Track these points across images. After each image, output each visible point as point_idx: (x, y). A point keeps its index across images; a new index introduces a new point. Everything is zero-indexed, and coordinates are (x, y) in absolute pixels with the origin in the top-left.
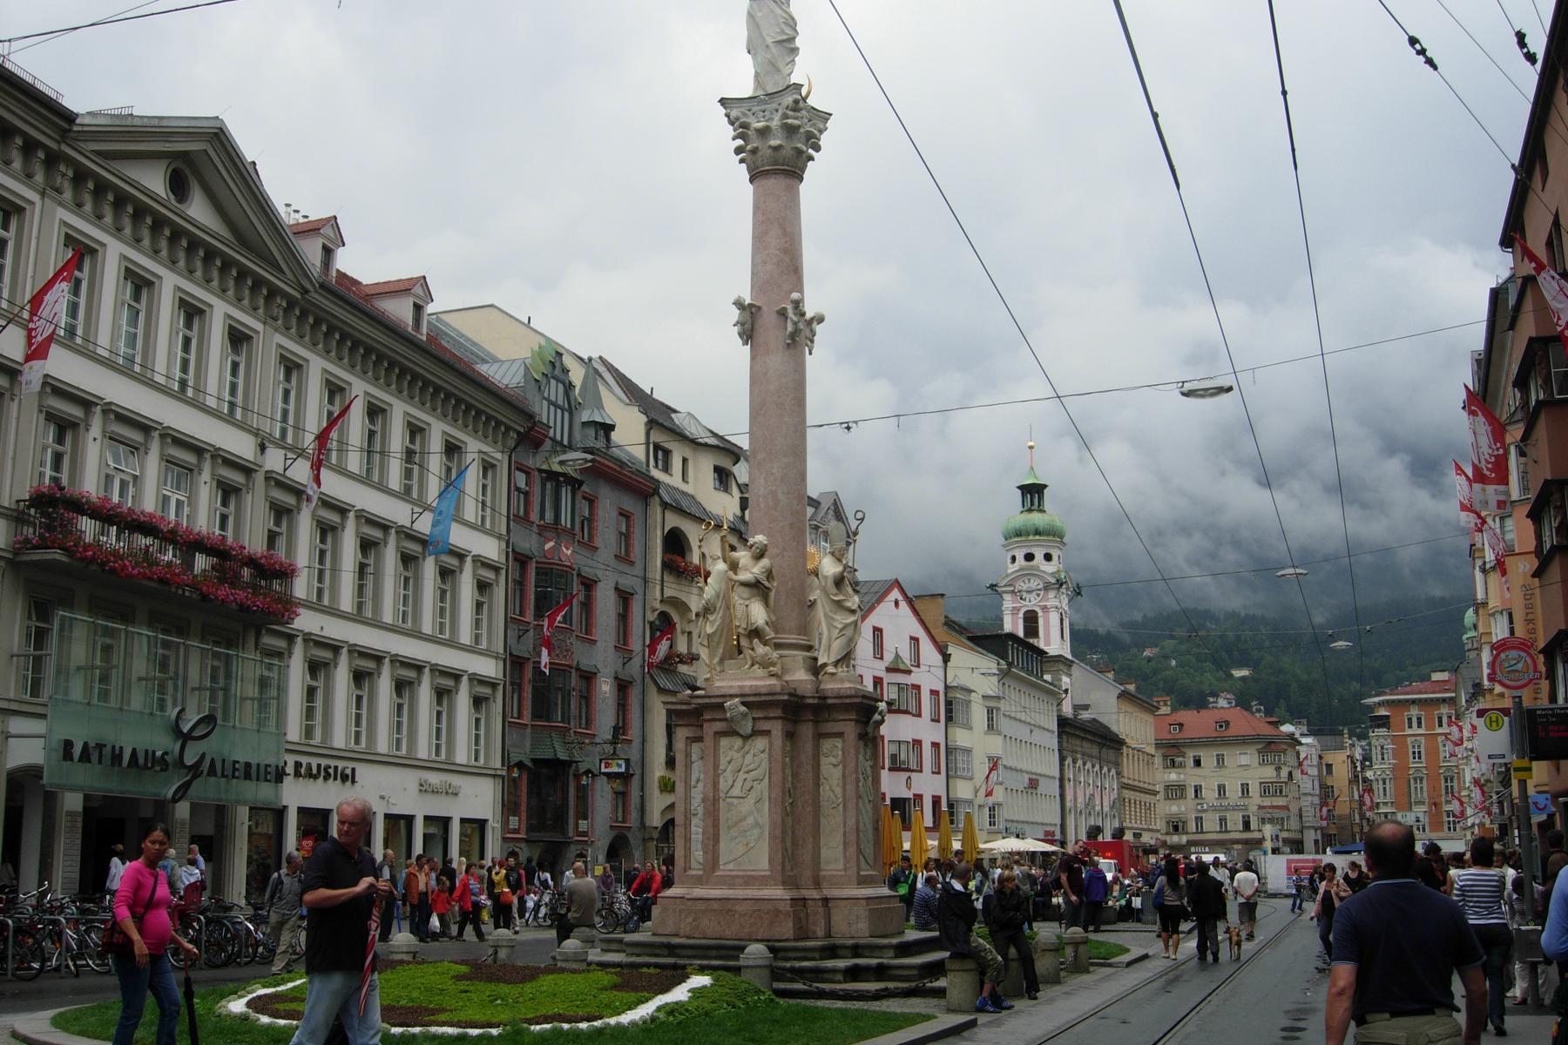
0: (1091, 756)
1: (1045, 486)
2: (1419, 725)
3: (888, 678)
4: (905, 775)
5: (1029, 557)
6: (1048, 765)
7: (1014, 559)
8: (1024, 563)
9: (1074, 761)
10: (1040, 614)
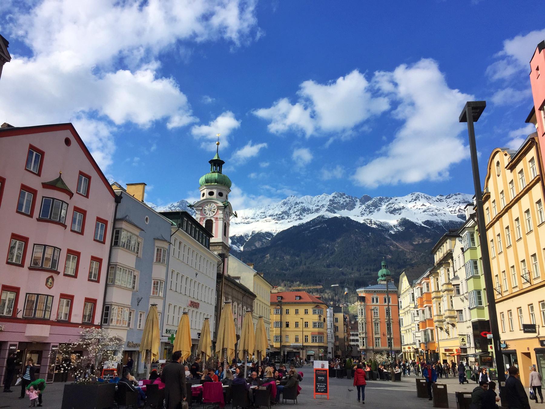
0: (238, 299)
1: (223, 162)
2: (377, 302)
3: (42, 193)
4: (48, 274)
5: (211, 194)
6: (208, 297)
7: (203, 195)
8: (209, 197)
9: (227, 299)
10: (214, 221)
